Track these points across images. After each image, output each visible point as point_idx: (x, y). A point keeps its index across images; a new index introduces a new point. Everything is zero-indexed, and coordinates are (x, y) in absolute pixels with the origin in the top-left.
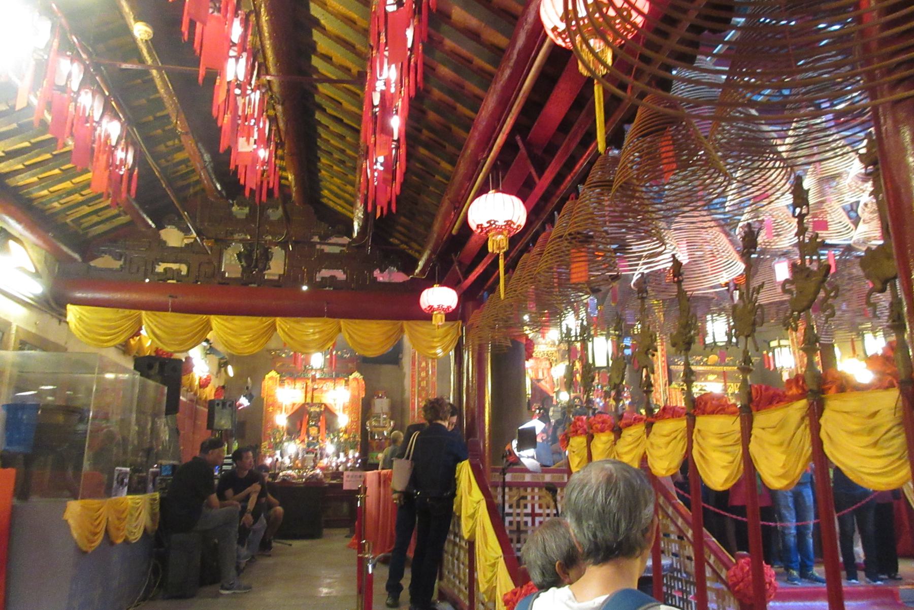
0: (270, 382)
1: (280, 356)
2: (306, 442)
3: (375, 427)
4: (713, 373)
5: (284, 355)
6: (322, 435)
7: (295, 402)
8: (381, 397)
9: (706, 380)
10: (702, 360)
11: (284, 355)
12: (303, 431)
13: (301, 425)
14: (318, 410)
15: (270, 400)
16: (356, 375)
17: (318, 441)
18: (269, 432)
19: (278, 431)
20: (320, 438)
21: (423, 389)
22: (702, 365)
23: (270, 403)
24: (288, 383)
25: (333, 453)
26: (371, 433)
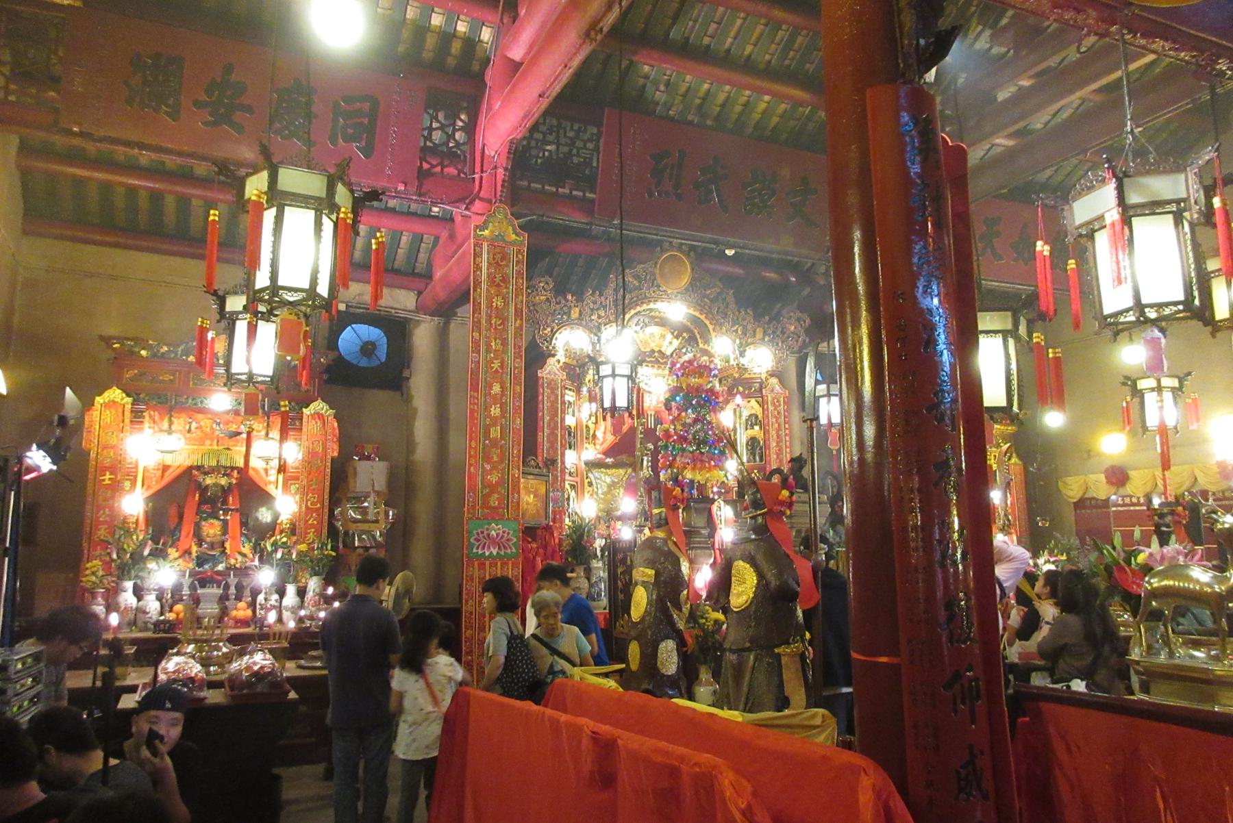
0: (108, 416)
1: (133, 354)
2: (194, 555)
3: (356, 521)
5: (143, 353)
6: (233, 538)
7: (168, 462)
8: (368, 458)
11: (143, 353)
12: (187, 528)
13: (181, 517)
14: (223, 481)
15: (107, 458)
16: (318, 406)
17: (223, 552)
18: (102, 533)
19: (128, 533)
20: (227, 545)
21: (494, 443)
23: (107, 462)
24: (152, 418)
25: (273, 585)
26: (346, 533)
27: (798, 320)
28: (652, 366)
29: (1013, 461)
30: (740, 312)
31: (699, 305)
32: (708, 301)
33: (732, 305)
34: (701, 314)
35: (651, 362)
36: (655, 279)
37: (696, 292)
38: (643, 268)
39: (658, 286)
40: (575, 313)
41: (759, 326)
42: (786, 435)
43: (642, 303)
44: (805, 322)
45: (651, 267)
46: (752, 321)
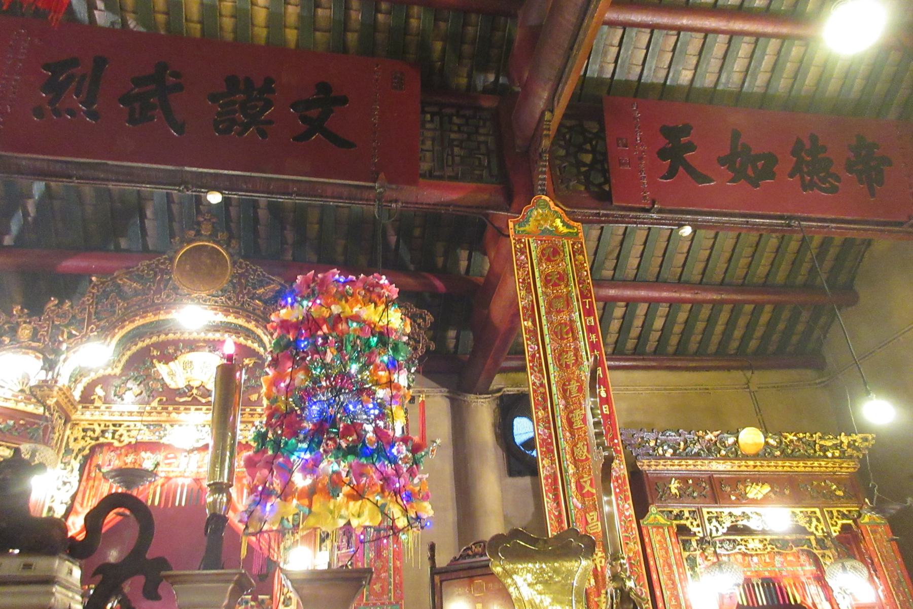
4: (758, 479)
9: (742, 499)
22: (725, 458)
28: (186, 409)
29: (866, 519)
31: (246, 310)
34: (249, 322)
35: (184, 403)
36: (171, 278)
37: (241, 292)
38: (148, 266)
39: (175, 289)
40: (25, 332)
43: (147, 312)
44: (424, 320)
45: (162, 263)
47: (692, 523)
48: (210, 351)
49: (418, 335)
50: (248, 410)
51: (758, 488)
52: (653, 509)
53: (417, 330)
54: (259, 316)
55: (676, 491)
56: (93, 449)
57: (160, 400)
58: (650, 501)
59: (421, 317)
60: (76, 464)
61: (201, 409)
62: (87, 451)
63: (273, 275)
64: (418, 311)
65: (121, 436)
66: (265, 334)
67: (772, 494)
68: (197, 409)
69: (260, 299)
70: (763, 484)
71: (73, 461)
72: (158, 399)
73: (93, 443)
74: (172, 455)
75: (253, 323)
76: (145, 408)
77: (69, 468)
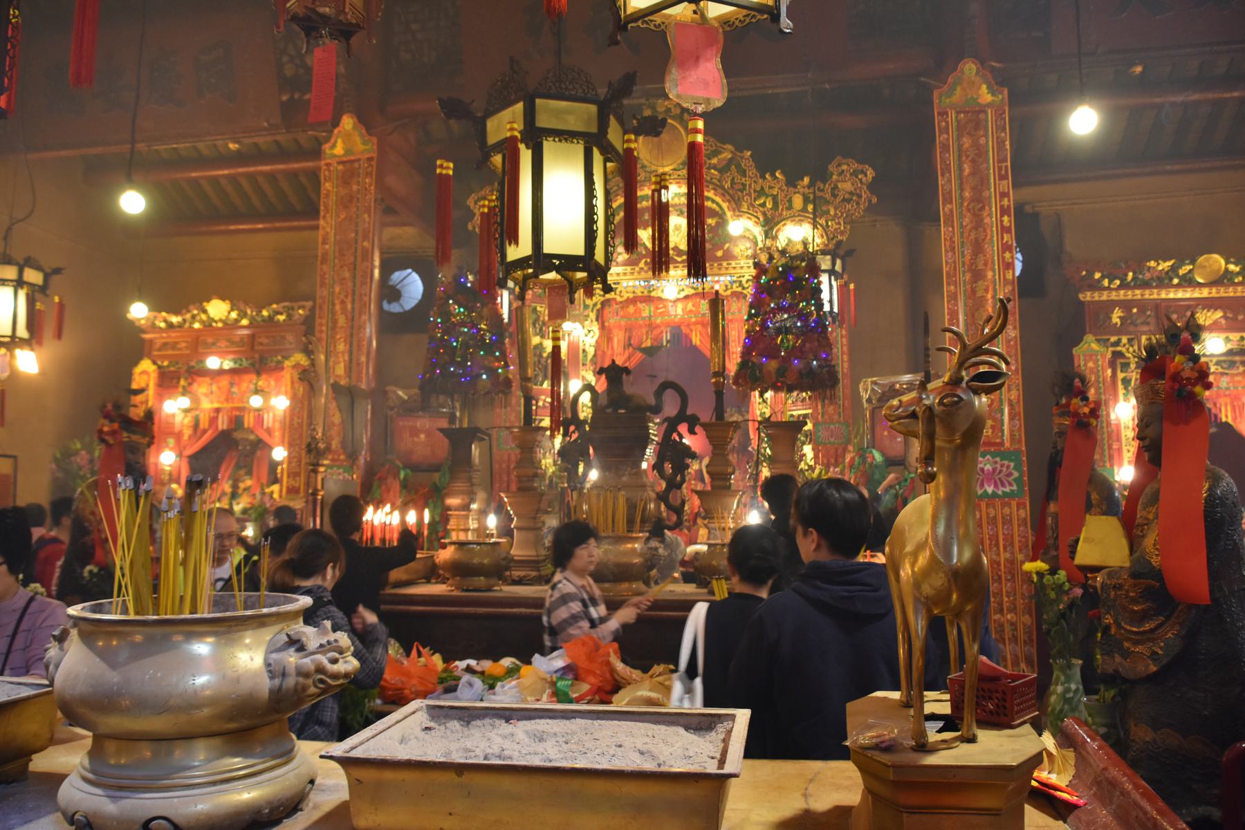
10: (1174, 269)
22: (1179, 286)
27: (855, 174)
30: (764, 178)
32: (716, 173)
33: (752, 172)
41: (795, 193)
42: (842, 337)
44: (866, 176)
46: (784, 187)
47: (1128, 349)
48: (678, 215)
49: (861, 191)
50: (716, 265)
51: (1209, 314)
52: (1089, 338)
53: (859, 185)
54: (717, 186)
55: (1118, 321)
56: (603, 303)
57: (646, 262)
58: (1088, 329)
59: (862, 172)
60: (593, 316)
61: (678, 267)
62: (599, 306)
63: (724, 144)
64: (860, 167)
65: (621, 292)
66: (723, 201)
67: (1223, 321)
68: (675, 267)
69: (715, 168)
70: (1216, 310)
71: (591, 314)
72: (644, 260)
73: (602, 299)
74: (661, 306)
75: (712, 192)
76: (634, 269)
77: (589, 320)
